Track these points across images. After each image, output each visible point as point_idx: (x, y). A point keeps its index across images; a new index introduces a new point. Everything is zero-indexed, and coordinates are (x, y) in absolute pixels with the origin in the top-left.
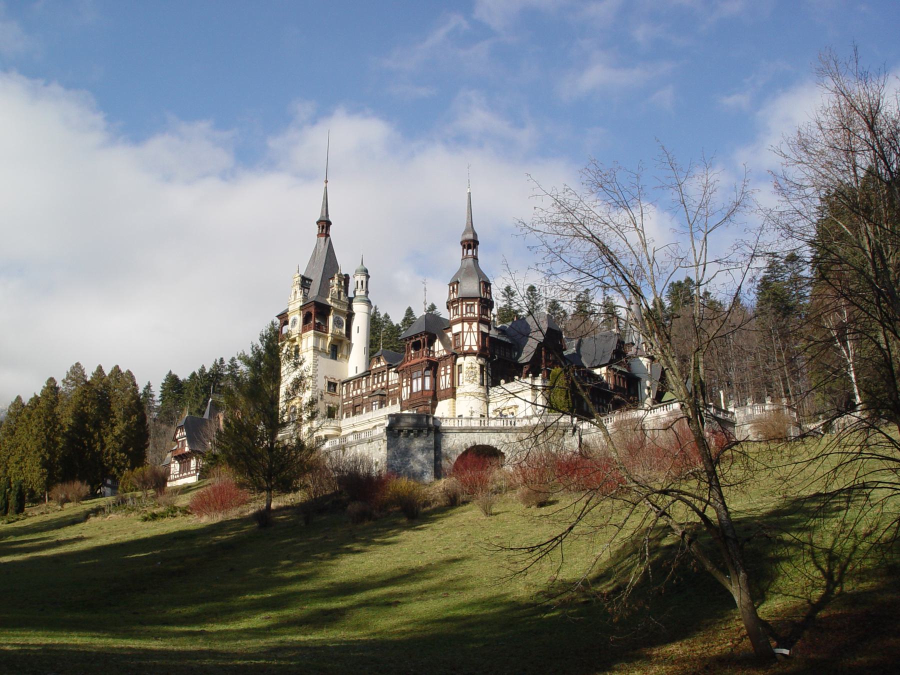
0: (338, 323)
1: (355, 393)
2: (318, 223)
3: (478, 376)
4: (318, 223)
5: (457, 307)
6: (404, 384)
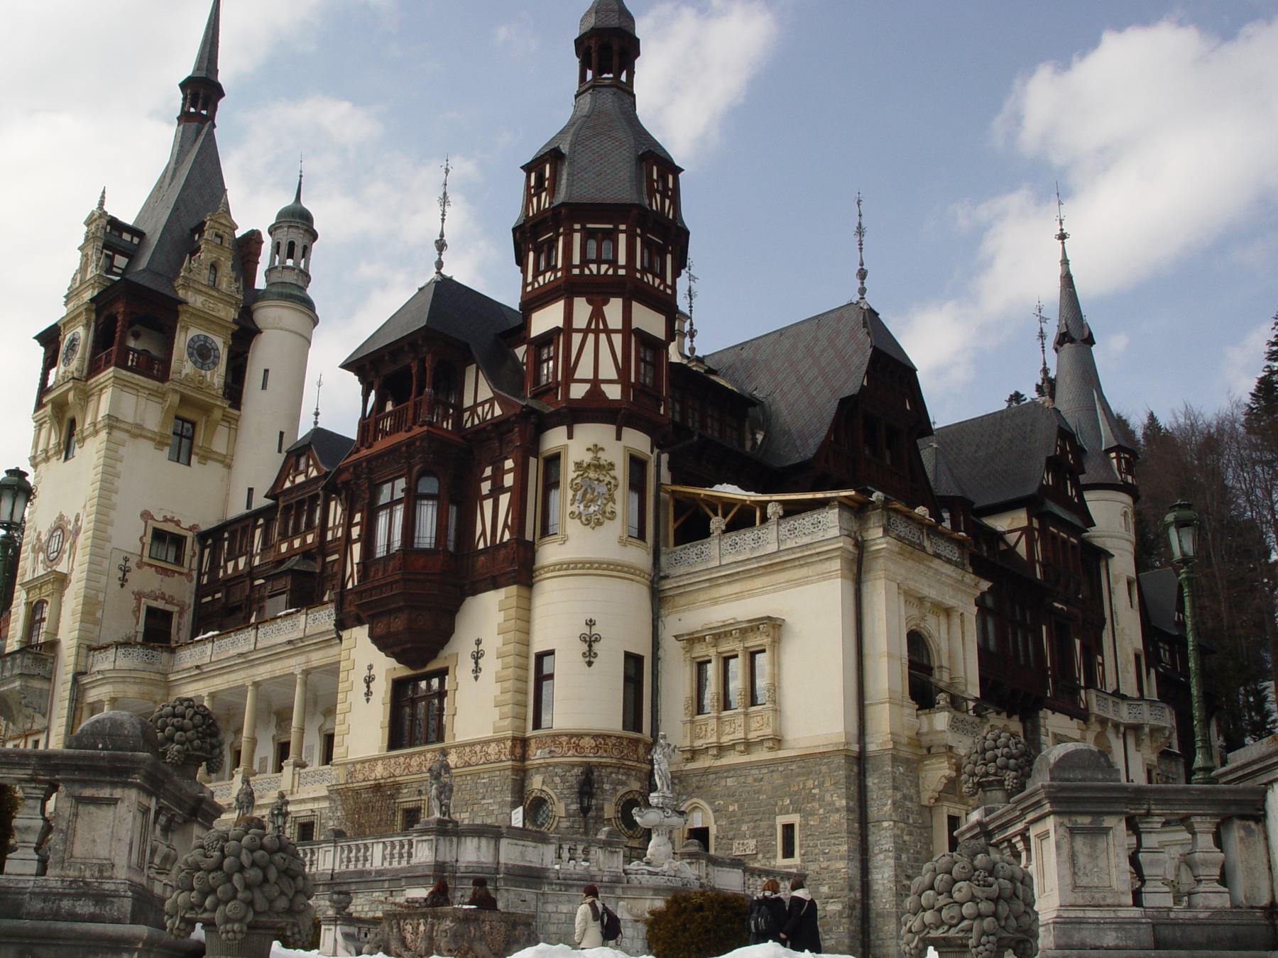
0: (202, 353)
2: (184, 86)
3: (619, 494)
4: (184, 86)
5: (552, 244)
6: (355, 532)
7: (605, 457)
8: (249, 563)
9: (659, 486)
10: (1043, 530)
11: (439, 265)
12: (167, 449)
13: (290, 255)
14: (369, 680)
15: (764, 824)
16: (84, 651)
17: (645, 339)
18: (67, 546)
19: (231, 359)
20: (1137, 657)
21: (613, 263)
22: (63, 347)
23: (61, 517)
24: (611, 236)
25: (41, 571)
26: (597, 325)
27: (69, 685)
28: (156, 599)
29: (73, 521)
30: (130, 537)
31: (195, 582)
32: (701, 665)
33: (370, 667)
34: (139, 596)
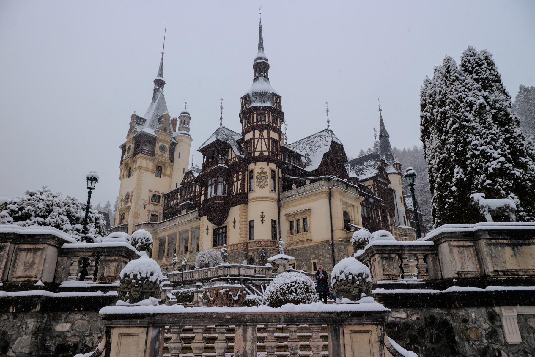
0: (163, 149)
2: (154, 81)
4: (154, 81)
5: (249, 118)
6: (203, 192)
7: (264, 170)
8: (177, 201)
9: (279, 177)
10: (377, 185)
11: (221, 124)
13: (184, 123)
14: (207, 230)
15: (308, 262)
17: (273, 140)
19: (171, 150)
20: (404, 217)
21: (265, 121)
22: (127, 149)
24: (264, 114)
26: (261, 137)
30: (146, 196)
32: (291, 223)
33: (208, 226)
34: (149, 211)
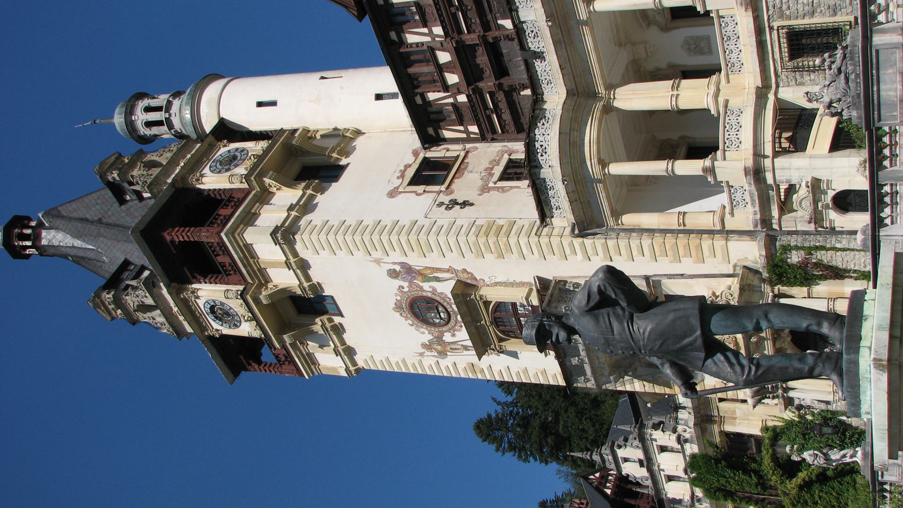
1: (452, 78)
12: (325, 185)
16: (546, 230)
18: (426, 286)
22: (226, 331)
23: (398, 307)
25: (463, 335)
27: (588, 242)
28: (492, 175)
29: (398, 283)
31: (477, 145)
34: (485, 189)
